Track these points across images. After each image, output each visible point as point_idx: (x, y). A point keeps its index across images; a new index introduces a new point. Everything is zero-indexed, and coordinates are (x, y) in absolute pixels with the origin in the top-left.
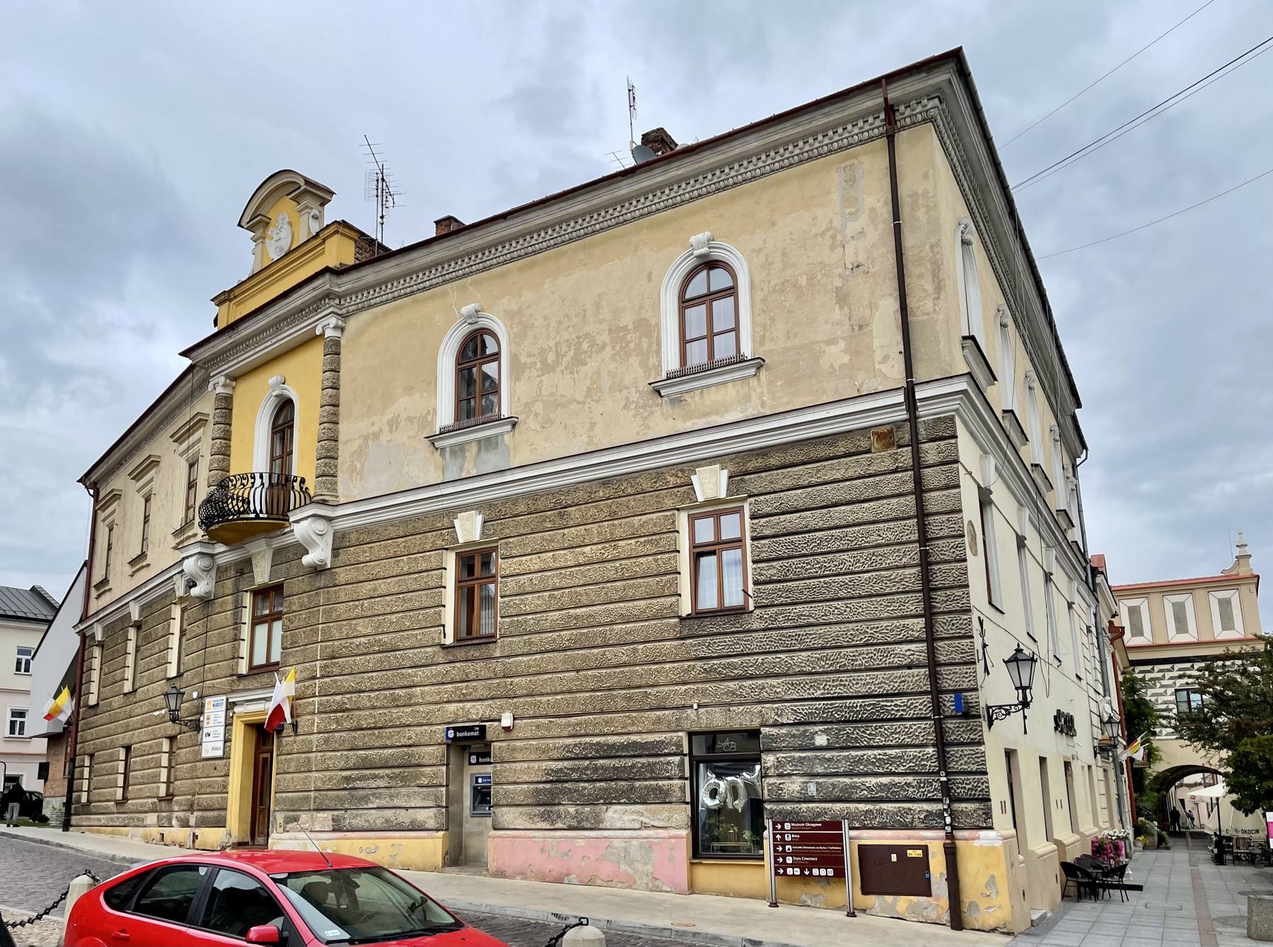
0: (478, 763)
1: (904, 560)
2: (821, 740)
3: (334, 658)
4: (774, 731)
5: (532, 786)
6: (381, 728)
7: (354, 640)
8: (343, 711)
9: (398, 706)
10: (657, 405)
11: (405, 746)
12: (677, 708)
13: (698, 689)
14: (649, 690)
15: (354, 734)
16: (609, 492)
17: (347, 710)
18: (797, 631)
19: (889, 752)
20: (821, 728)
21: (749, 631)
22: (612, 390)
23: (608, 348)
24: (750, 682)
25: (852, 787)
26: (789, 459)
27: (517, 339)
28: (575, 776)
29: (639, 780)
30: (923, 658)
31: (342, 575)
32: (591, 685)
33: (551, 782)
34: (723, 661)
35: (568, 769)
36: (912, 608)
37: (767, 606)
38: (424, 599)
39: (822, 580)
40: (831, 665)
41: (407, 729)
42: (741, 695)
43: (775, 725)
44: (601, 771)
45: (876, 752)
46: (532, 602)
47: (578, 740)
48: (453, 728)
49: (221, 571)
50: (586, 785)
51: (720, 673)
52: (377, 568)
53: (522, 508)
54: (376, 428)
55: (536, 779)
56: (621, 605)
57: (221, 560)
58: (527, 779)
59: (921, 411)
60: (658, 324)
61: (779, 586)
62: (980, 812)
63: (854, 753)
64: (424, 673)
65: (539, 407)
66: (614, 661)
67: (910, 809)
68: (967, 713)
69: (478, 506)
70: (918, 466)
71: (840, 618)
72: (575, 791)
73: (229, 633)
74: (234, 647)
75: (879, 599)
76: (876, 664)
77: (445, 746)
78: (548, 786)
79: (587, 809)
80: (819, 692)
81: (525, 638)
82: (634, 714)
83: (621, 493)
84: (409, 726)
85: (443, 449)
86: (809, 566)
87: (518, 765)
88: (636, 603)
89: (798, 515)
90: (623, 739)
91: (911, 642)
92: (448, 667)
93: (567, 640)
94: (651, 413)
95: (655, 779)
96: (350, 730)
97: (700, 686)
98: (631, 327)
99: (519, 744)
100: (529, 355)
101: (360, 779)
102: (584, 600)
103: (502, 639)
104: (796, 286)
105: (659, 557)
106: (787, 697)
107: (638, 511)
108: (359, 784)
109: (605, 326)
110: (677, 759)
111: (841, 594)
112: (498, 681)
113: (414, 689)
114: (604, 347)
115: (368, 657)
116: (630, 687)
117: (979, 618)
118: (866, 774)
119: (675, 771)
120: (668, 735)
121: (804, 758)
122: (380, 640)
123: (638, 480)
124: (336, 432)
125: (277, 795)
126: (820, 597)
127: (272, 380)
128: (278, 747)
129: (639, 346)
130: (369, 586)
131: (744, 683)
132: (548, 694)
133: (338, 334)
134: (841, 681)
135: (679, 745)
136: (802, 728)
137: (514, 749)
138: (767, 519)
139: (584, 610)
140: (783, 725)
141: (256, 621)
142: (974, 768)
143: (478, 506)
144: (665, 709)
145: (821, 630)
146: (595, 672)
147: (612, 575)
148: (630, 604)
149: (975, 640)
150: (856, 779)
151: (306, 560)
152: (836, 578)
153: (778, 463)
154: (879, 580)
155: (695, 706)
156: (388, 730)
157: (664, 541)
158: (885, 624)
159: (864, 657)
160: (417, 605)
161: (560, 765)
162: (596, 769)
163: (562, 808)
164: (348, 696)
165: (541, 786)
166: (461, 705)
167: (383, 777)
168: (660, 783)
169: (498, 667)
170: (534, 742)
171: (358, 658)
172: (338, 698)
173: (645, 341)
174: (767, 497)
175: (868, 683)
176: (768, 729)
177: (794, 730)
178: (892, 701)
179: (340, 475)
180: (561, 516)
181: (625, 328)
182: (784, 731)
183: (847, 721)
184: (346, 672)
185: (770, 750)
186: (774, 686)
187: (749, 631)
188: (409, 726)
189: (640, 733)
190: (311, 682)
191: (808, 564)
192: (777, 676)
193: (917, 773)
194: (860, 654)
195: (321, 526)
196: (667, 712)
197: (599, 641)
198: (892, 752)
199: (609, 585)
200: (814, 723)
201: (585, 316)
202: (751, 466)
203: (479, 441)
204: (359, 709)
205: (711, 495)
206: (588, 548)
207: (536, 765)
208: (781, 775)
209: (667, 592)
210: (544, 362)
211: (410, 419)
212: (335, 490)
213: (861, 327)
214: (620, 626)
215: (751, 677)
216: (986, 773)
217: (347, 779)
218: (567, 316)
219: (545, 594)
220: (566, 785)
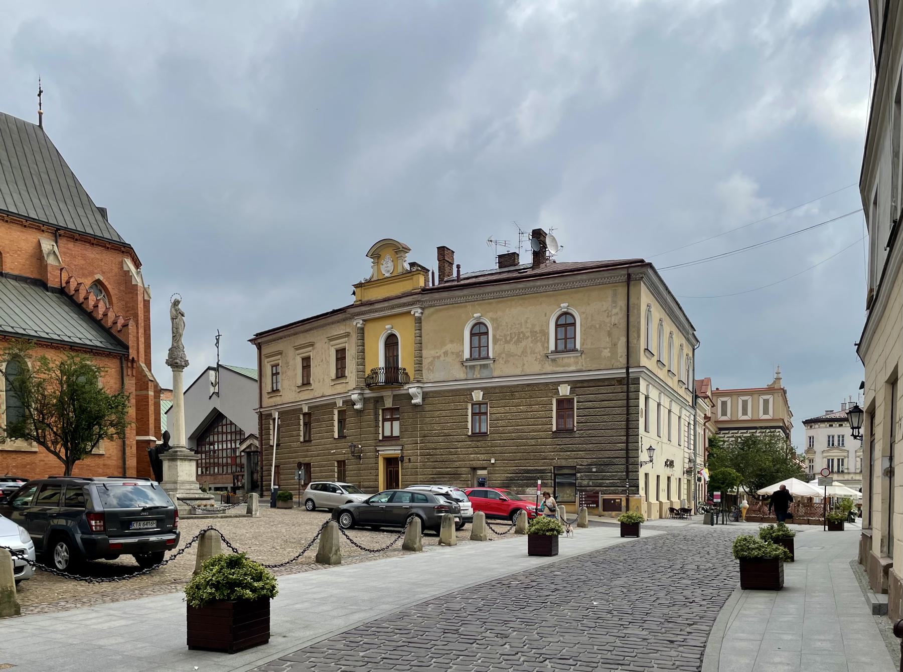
2: (594, 470)
4: (581, 467)
16: (530, 388)
22: (531, 354)
23: (530, 339)
27: (495, 329)
28: (516, 479)
30: (625, 448)
32: (522, 451)
43: (581, 465)
49: (365, 400)
52: (440, 406)
53: (498, 391)
54: (438, 355)
57: (366, 396)
59: (630, 375)
65: (504, 355)
66: (530, 444)
69: (481, 389)
70: (628, 392)
73: (373, 423)
74: (376, 430)
85: (466, 366)
87: (497, 475)
90: (532, 468)
92: (470, 443)
94: (545, 363)
100: (500, 336)
101: (438, 478)
102: (520, 424)
104: (595, 327)
107: (539, 396)
108: (437, 480)
109: (529, 330)
110: (550, 474)
114: (528, 338)
119: (550, 478)
124: (421, 354)
127: (387, 327)
129: (541, 339)
130: (438, 413)
133: (420, 315)
135: (551, 470)
137: (496, 470)
140: (583, 465)
141: (384, 420)
143: (481, 389)
145: (597, 438)
146: (524, 447)
147: (530, 416)
151: (413, 401)
154: (614, 425)
159: (608, 447)
161: (511, 475)
162: (523, 477)
173: (543, 338)
177: (586, 467)
179: (423, 370)
180: (512, 395)
181: (536, 332)
183: (602, 465)
192: (583, 451)
195: (419, 390)
197: (525, 437)
203: (481, 365)
205: (564, 394)
208: (582, 479)
211: (452, 353)
212: (422, 376)
213: (615, 345)
215: (574, 451)
217: (433, 478)
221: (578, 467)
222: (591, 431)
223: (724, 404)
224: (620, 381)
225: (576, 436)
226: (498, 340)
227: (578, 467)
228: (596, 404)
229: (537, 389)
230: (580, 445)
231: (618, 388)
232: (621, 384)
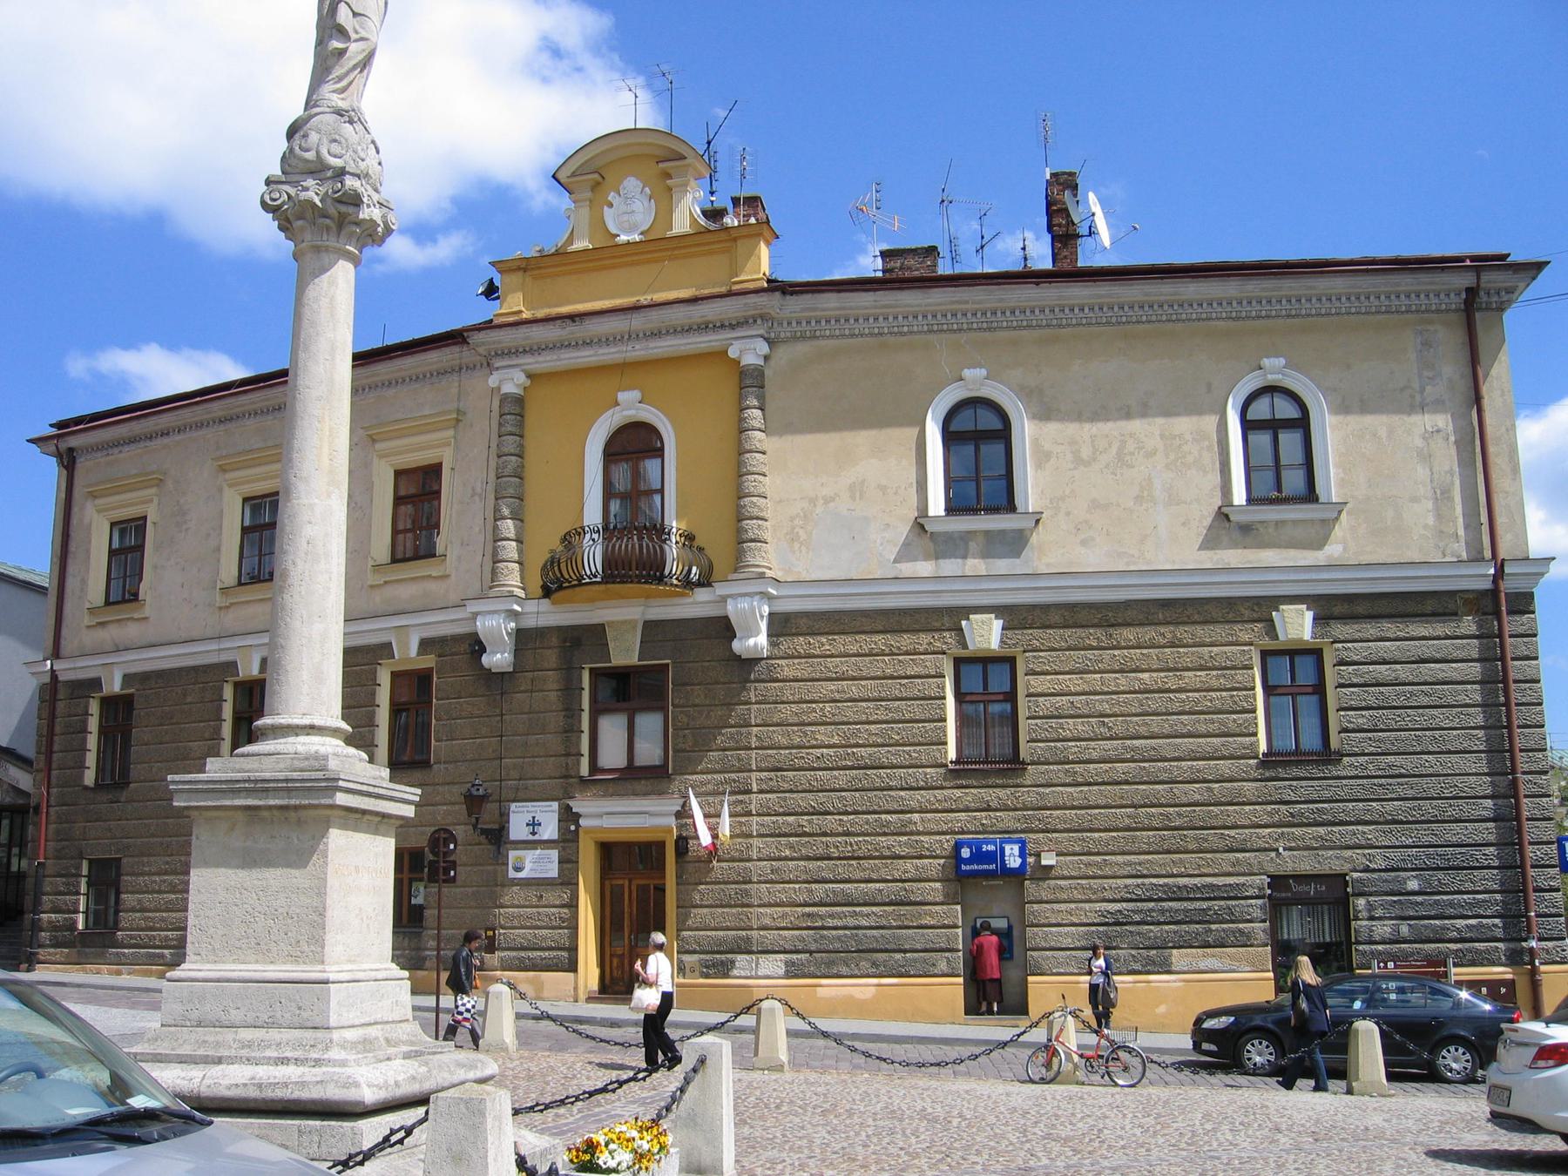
1: (1490, 721)
2: (1413, 885)
13: (1283, 833)
14: (1227, 832)
17: (805, 834)
18: (1390, 781)
25: (1443, 928)
28: (1137, 918)
29: (1214, 923)
34: (1311, 806)
38: (916, 709)
40: (1423, 815)
42: (1331, 841)
43: (1367, 870)
45: (1465, 897)
46: (1072, 726)
47: (1140, 881)
56: (1191, 740)
58: (1076, 920)
63: (1445, 897)
66: (1184, 800)
69: (998, 610)
72: (1139, 933)
73: (556, 720)
75: (1467, 756)
76: (1465, 816)
83: (1186, 619)
87: (1063, 907)
88: (1209, 740)
89: (1388, 666)
90: (1197, 881)
97: (1285, 830)
98: (1188, 437)
101: (832, 916)
102: (1143, 730)
105: (1235, 693)
108: (830, 922)
110: (1260, 902)
111: (1431, 749)
114: (1153, 453)
121: (1395, 902)
123: (1206, 608)
126: (1411, 750)
130: (832, 686)
132: (1099, 830)
138: (1356, 667)
140: (1374, 871)
143: (998, 610)
150: (1446, 922)
153: (1366, 613)
157: (1240, 675)
162: (1163, 911)
164: (806, 818)
165: (1093, 928)
167: (868, 915)
168: (1241, 926)
169: (1029, 796)
182: (1375, 875)
186: (1365, 833)
187: (1339, 778)
194: (1451, 806)
196: (1247, 855)
200: (1405, 870)
203: (987, 533)
204: (825, 834)
206: (1145, 676)
207: (1087, 906)
208: (1372, 918)
211: (883, 489)
221: (1355, 875)
222: (1391, 758)
225: (1344, 773)
226: (1048, 455)
228: (1403, 672)
229: (1196, 617)
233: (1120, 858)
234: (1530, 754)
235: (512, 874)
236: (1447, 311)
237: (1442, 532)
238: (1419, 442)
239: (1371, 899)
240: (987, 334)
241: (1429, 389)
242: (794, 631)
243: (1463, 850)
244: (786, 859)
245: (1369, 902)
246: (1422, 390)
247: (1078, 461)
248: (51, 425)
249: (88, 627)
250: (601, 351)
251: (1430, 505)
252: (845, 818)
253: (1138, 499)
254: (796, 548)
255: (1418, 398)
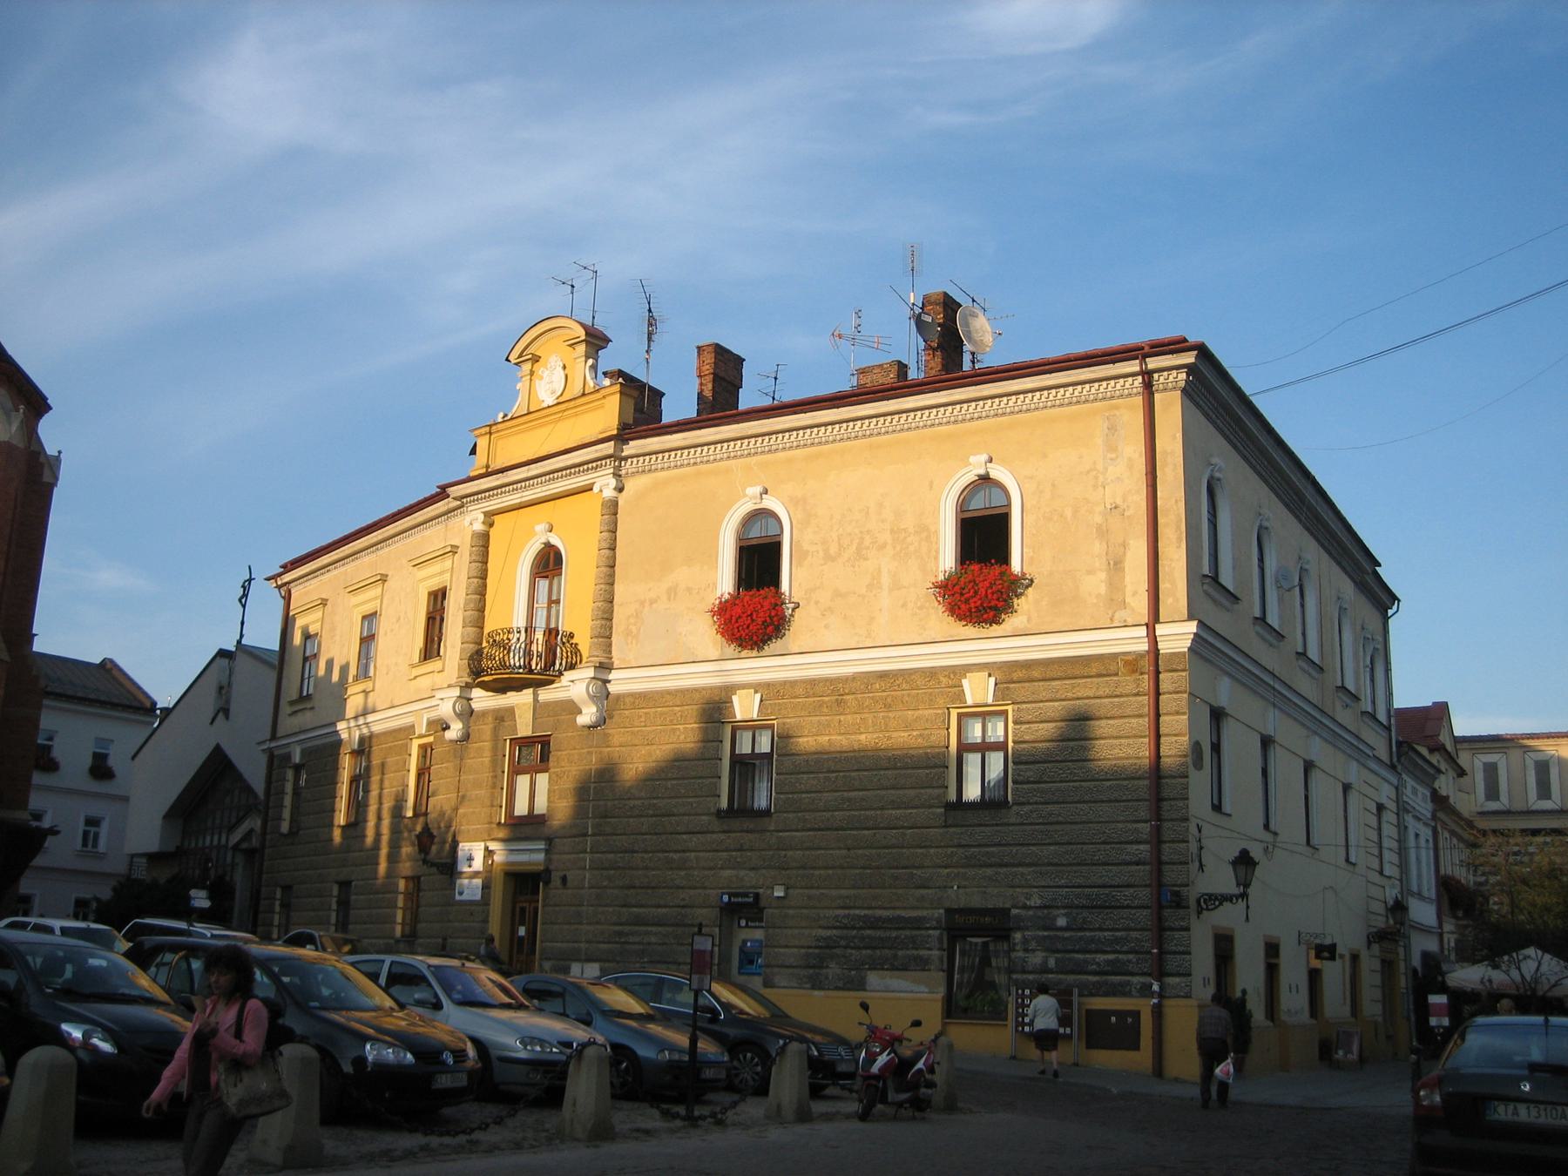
0: (747, 926)
2: (1062, 922)
3: (606, 817)
4: (1023, 912)
5: (803, 951)
6: (653, 888)
7: (627, 802)
8: (614, 869)
9: (671, 869)
10: (933, 608)
11: (679, 906)
12: (939, 888)
15: (626, 892)
18: (1047, 827)
19: (1117, 934)
20: (1063, 911)
21: (1009, 825)
24: (1005, 869)
25: (1085, 961)
26: (1049, 674)
29: (902, 949)
31: (616, 736)
33: (821, 947)
35: (837, 937)
36: (1142, 814)
37: (1023, 804)
39: (1071, 784)
40: (1075, 859)
41: (681, 891)
44: (867, 940)
45: (1106, 934)
47: (847, 912)
48: (727, 893)
50: (853, 951)
51: (979, 860)
55: (806, 944)
60: (936, 532)
61: (1035, 786)
62: (1183, 985)
63: (1088, 934)
64: (699, 839)
67: (1129, 981)
68: (1179, 902)
71: (1084, 818)
77: (718, 909)
78: (817, 951)
79: (853, 972)
80: (1063, 881)
81: (800, 814)
82: (900, 891)
84: (682, 888)
86: (1061, 772)
87: (789, 932)
88: (906, 791)
91: (1140, 843)
92: (722, 836)
93: (840, 820)
95: (917, 949)
96: (622, 888)
97: (962, 870)
99: (791, 912)
103: (778, 814)
106: (1035, 884)
108: (631, 939)
110: (936, 933)
111: (1087, 798)
112: (771, 853)
113: (688, 854)
114: (883, 547)
115: (642, 819)
116: (897, 868)
117: (1198, 825)
118: (1096, 952)
120: (930, 912)
122: (654, 805)
123: (913, 677)
125: (544, 944)
128: (544, 900)
131: (999, 870)
132: (819, 868)
134: (1081, 872)
136: (1046, 911)
138: (1028, 726)
139: (856, 793)
142: (1182, 949)
143: (757, 687)
144: (929, 888)
146: (867, 852)
148: (901, 792)
149: (1190, 845)
152: (1083, 784)
153: (1040, 677)
155: (955, 887)
156: (661, 891)
158: (1120, 825)
160: (693, 774)
161: (829, 933)
163: (828, 970)
165: (811, 951)
166: (734, 872)
170: (805, 911)
171: (631, 820)
172: (611, 856)
174: (1029, 706)
175: (1103, 876)
176: (1017, 911)
177: (1039, 913)
178: (1121, 892)
180: (839, 703)
181: (905, 530)
182: (1031, 913)
183: (1083, 907)
184: (619, 832)
185: (1019, 929)
187: (1009, 825)
188: (682, 888)
189: (905, 908)
190: (581, 839)
191: (1061, 769)
193: (1137, 952)
196: (930, 891)
198: (1119, 934)
199: (882, 772)
200: (1058, 908)
201: (868, 513)
202: (1015, 676)
207: (807, 932)
208: (1026, 950)
209: (935, 784)
210: (826, 551)
211: (689, 589)
214: (890, 811)
215: (1006, 865)
216: (1190, 953)
217: (620, 934)
218: (851, 511)
219: (820, 775)
220: (834, 951)
222: (1050, 807)
223: (1491, 770)
224: (1131, 663)
225: (1013, 820)
227: (1014, 911)
230: (1024, 849)
231: (1128, 683)
232: (1134, 671)
233: (834, 892)
234: (1173, 803)
235: (458, 897)
236: (1130, 395)
237: (1112, 600)
238: (1098, 519)
239: (1026, 933)
240: (769, 456)
241: (1110, 468)
242: (622, 707)
243: (1107, 891)
244: (606, 887)
245: (1024, 936)
246: (1106, 469)
247: (829, 558)
248: (281, 567)
249: (290, 715)
250: (524, 494)
251: (1103, 575)
252: (646, 856)
253: (870, 587)
254: (629, 642)
255: (1101, 479)
